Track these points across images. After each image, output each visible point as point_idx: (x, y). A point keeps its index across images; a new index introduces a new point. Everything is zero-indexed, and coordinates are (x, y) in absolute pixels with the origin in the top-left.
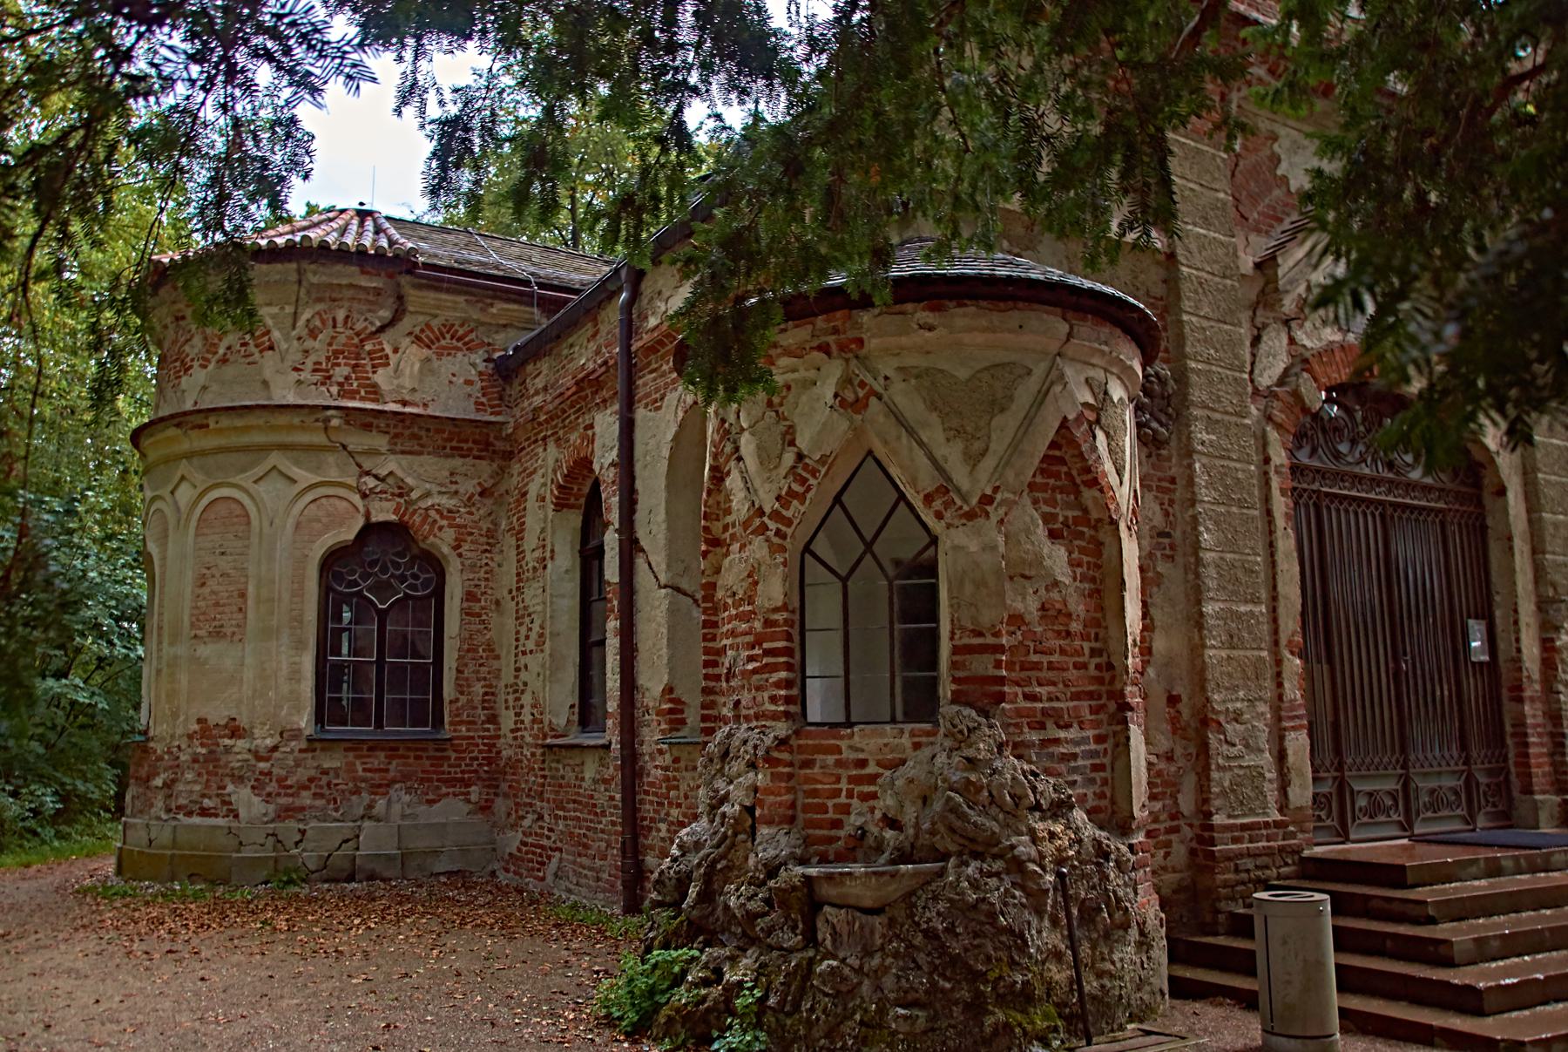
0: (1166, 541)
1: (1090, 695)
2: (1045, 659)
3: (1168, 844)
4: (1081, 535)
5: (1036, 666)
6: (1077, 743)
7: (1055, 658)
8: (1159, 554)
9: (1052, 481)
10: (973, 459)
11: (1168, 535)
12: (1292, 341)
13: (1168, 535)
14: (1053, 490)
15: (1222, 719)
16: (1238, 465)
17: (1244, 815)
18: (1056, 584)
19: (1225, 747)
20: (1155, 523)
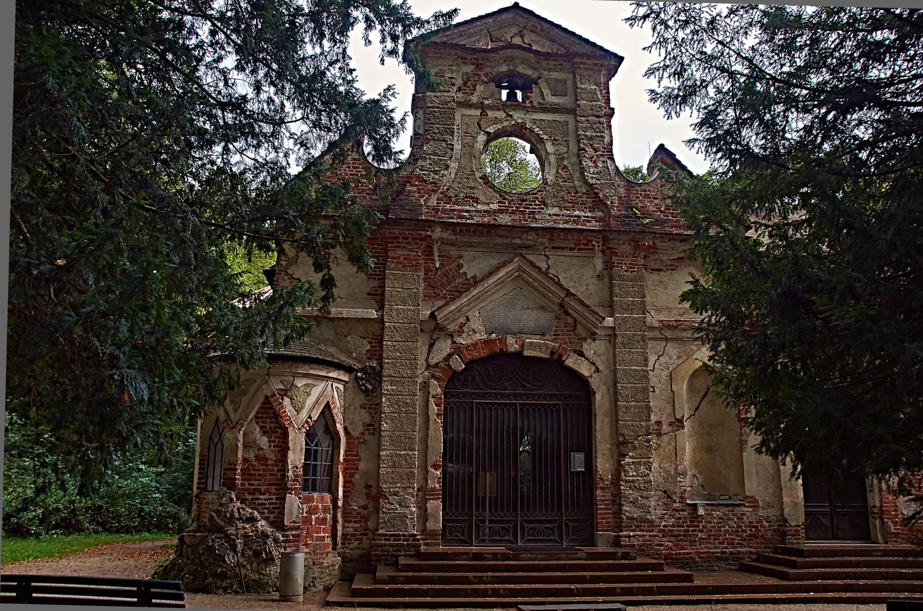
0: (372, 428)
1: (275, 485)
2: (257, 473)
3: (362, 539)
4: (277, 432)
5: (254, 475)
6: (266, 499)
7: (261, 472)
8: (367, 433)
9: (265, 416)
10: (235, 410)
11: (373, 425)
12: (454, 342)
13: (373, 425)
14: (266, 418)
15: (387, 494)
16: (407, 397)
17: (395, 531)
18: (262, 449)
19: (388, 505)
20: (366, 421)
